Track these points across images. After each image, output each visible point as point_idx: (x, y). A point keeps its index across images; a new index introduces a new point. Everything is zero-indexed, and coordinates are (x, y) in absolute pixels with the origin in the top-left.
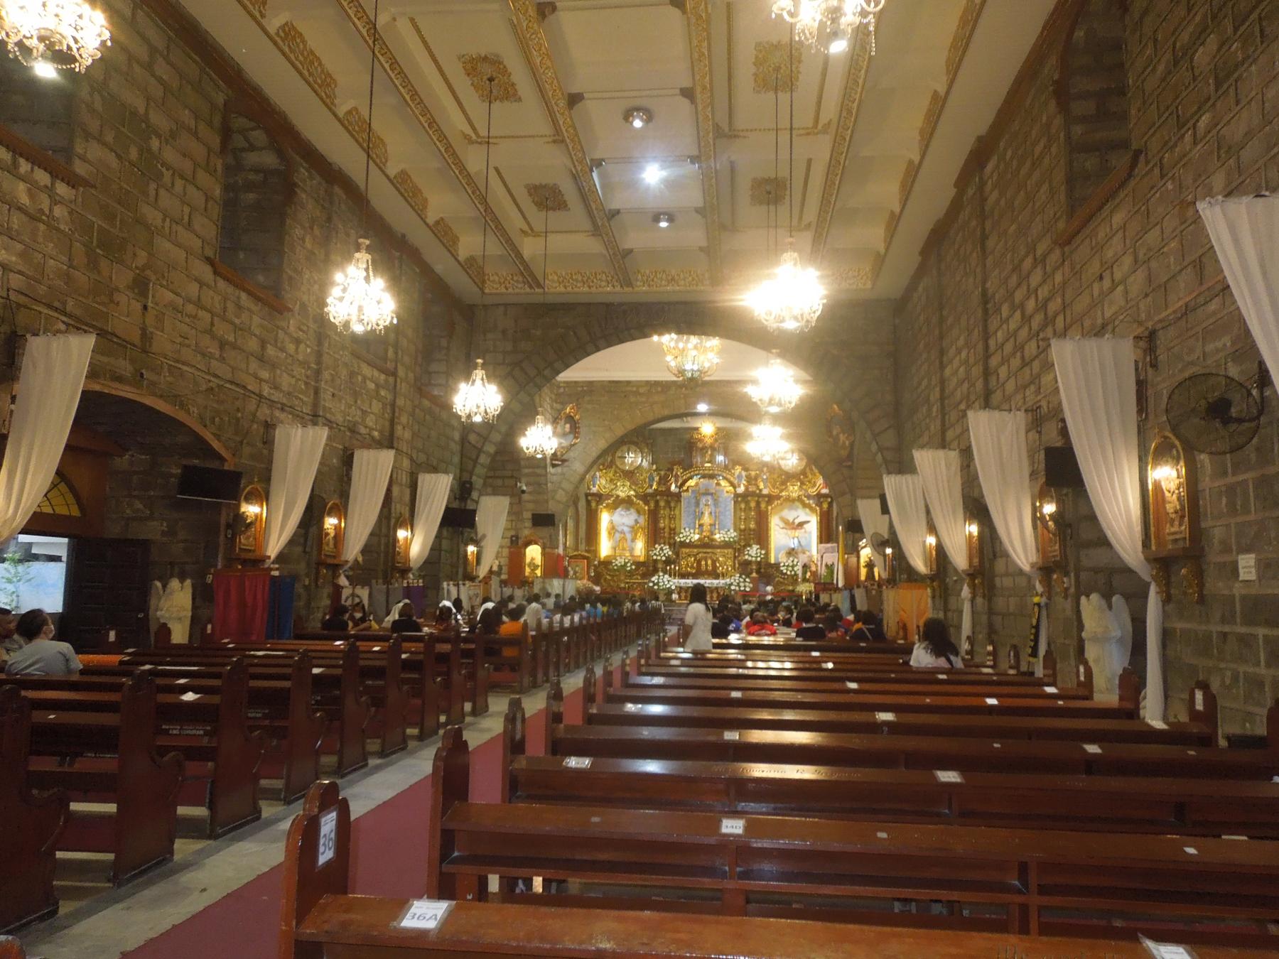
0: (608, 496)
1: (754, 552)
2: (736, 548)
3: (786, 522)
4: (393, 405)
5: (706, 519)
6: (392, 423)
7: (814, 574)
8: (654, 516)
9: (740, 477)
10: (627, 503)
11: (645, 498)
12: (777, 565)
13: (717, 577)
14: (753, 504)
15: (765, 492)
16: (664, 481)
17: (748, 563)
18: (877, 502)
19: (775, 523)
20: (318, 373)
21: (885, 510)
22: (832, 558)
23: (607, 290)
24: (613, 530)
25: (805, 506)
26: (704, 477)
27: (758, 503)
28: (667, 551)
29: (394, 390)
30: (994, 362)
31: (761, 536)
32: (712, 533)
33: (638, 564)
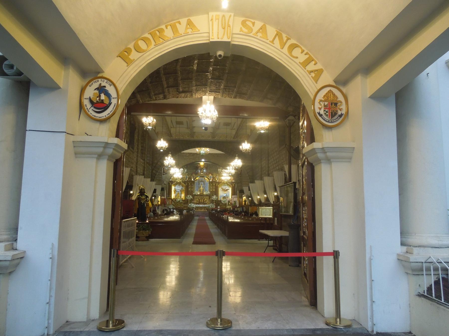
0: (175, 182)
1: (214, 197)
2: (209, 196)
3: (223, 189)
4: (144, 167)
5: (202, 188)
6: (144, 171)
7: (231, 203)
8: (187, 187)
9: (211, 177)
10: (179, 184)
11: (185, 182)
12: (221, 201)
13: (204, 204)
14: (214, 185)
15: (217, 181)
16: (190, 178)
17: (213, 200)
18: (248, 188)
19: (220, 189)
20: (137, 163)
21: (249, 190)
22: (235, 199)
23: (187, 138)
24: (175, 191)
25: (228, 185)
26: (201, 177)
27: (216, 184)
28: (191, 197)
29: (144, 164)
30: (270, 165)
31: (216, 193)
32: (203, 192)
33: (183, 200)
